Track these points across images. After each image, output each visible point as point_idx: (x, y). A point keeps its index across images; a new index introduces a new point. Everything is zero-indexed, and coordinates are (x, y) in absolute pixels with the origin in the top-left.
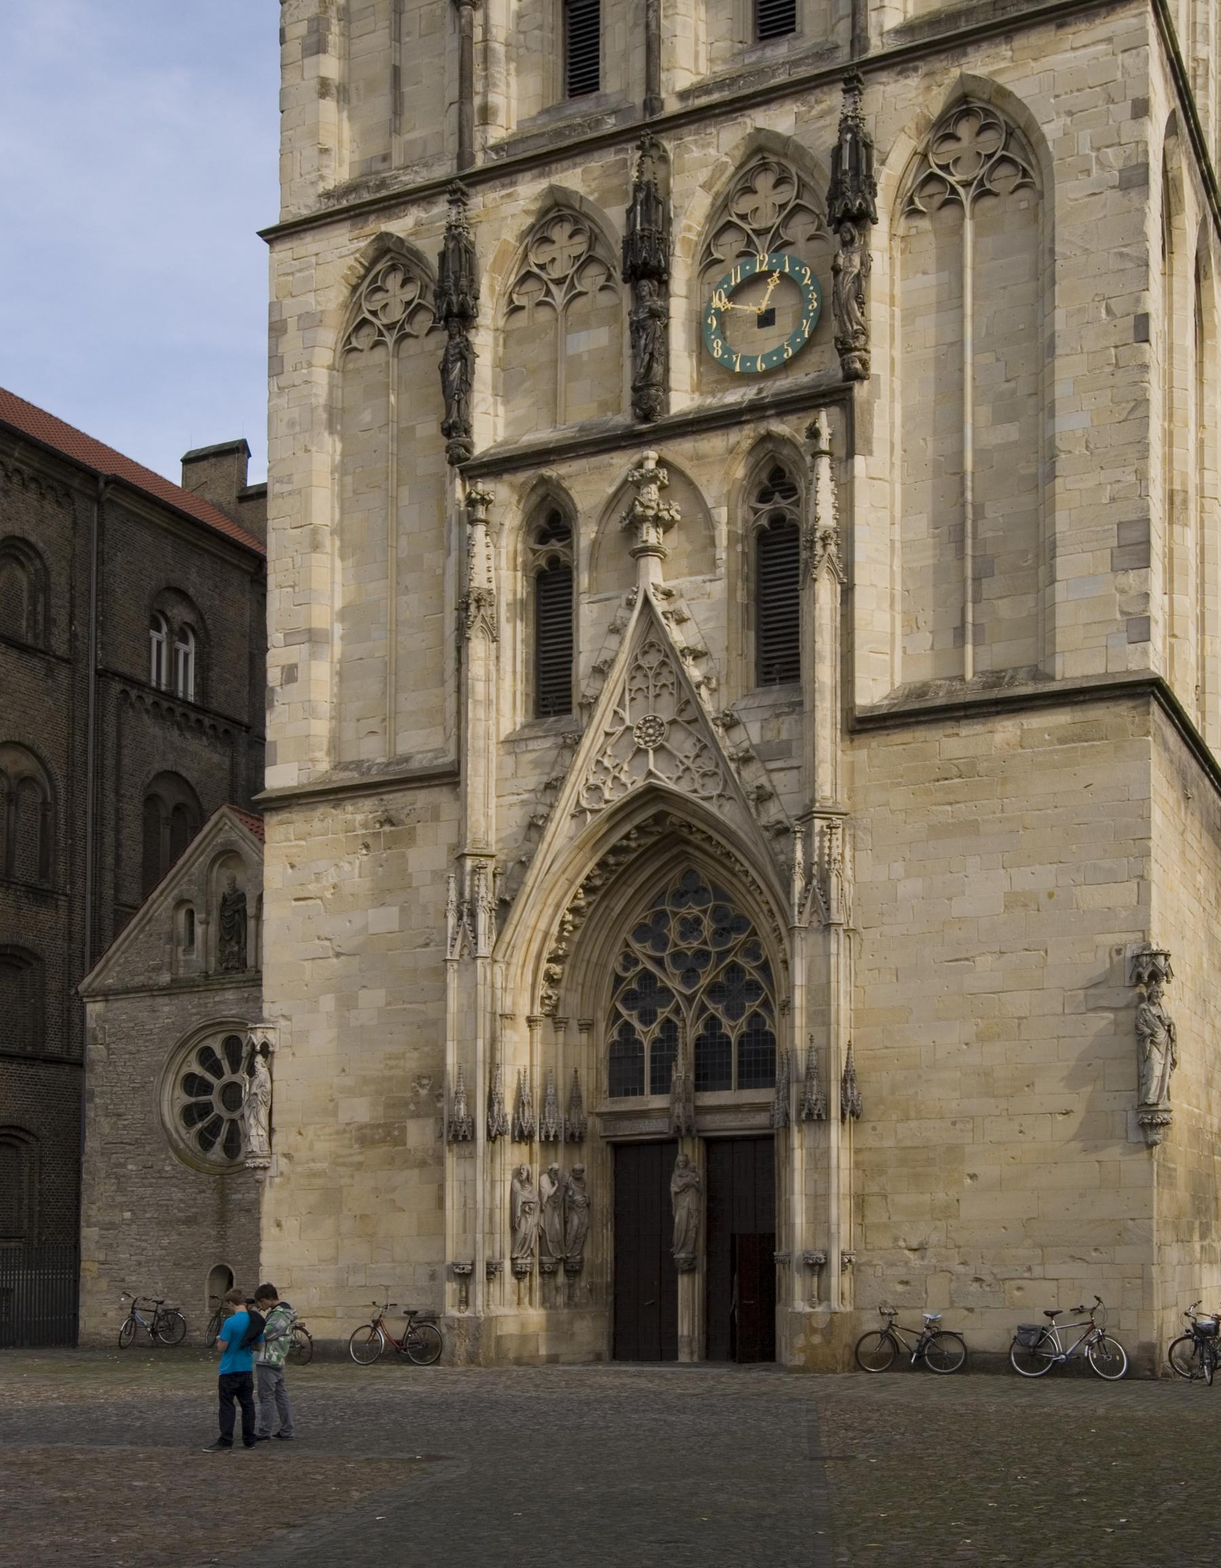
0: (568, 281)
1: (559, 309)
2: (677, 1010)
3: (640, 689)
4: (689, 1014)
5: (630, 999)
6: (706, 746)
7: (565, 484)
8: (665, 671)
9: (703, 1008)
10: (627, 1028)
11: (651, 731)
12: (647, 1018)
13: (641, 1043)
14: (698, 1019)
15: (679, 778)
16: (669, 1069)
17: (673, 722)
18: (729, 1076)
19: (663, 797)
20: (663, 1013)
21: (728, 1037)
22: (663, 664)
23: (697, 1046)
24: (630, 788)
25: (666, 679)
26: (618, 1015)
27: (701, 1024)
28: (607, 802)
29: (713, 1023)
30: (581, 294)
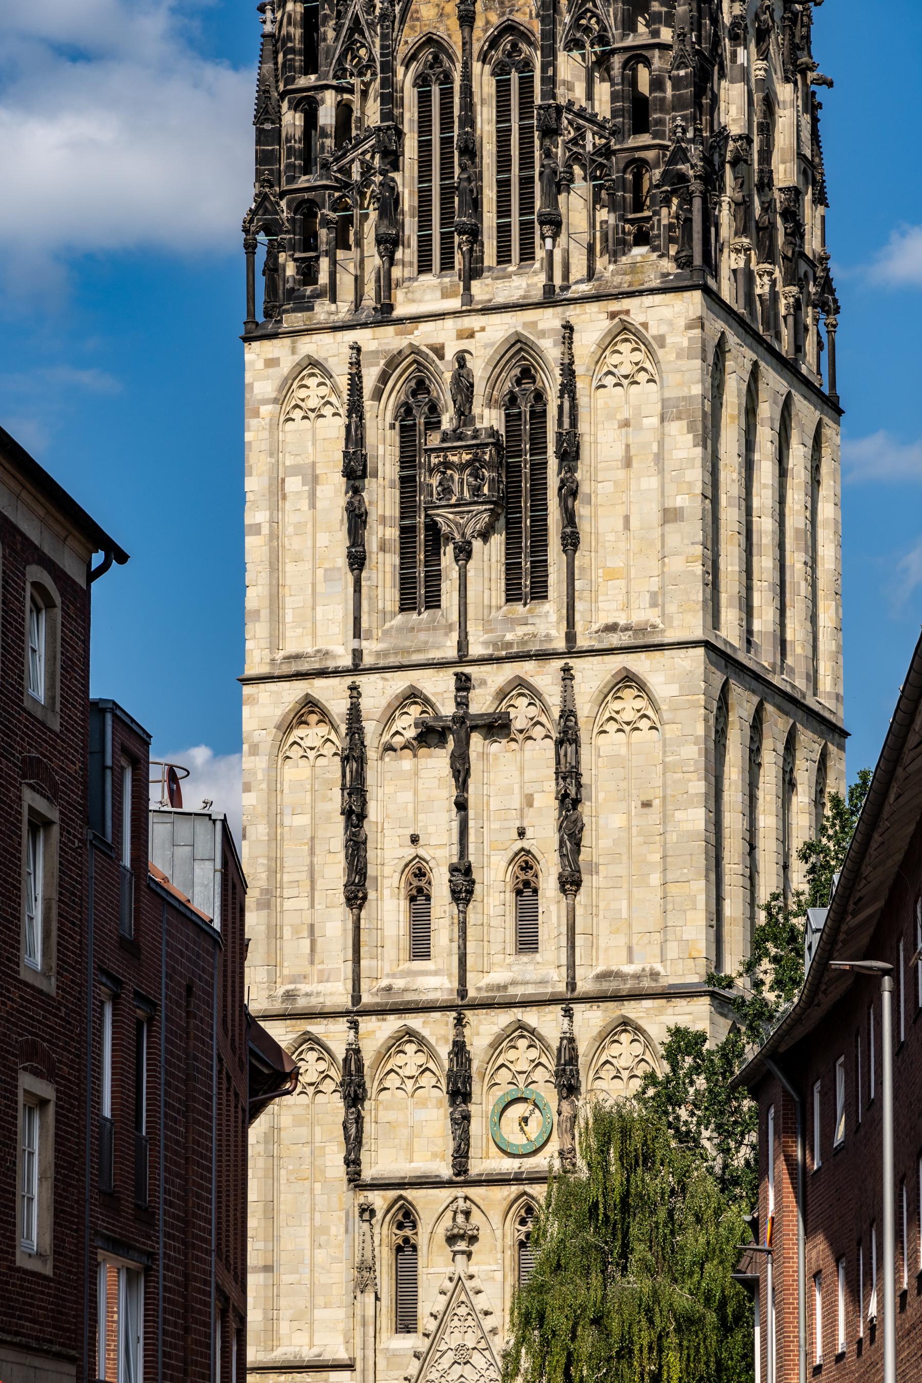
7: (414, 1203)
8: (469, 1317)
17: (474, 1349)
22: (469, 1314)
25: (470, 1322)
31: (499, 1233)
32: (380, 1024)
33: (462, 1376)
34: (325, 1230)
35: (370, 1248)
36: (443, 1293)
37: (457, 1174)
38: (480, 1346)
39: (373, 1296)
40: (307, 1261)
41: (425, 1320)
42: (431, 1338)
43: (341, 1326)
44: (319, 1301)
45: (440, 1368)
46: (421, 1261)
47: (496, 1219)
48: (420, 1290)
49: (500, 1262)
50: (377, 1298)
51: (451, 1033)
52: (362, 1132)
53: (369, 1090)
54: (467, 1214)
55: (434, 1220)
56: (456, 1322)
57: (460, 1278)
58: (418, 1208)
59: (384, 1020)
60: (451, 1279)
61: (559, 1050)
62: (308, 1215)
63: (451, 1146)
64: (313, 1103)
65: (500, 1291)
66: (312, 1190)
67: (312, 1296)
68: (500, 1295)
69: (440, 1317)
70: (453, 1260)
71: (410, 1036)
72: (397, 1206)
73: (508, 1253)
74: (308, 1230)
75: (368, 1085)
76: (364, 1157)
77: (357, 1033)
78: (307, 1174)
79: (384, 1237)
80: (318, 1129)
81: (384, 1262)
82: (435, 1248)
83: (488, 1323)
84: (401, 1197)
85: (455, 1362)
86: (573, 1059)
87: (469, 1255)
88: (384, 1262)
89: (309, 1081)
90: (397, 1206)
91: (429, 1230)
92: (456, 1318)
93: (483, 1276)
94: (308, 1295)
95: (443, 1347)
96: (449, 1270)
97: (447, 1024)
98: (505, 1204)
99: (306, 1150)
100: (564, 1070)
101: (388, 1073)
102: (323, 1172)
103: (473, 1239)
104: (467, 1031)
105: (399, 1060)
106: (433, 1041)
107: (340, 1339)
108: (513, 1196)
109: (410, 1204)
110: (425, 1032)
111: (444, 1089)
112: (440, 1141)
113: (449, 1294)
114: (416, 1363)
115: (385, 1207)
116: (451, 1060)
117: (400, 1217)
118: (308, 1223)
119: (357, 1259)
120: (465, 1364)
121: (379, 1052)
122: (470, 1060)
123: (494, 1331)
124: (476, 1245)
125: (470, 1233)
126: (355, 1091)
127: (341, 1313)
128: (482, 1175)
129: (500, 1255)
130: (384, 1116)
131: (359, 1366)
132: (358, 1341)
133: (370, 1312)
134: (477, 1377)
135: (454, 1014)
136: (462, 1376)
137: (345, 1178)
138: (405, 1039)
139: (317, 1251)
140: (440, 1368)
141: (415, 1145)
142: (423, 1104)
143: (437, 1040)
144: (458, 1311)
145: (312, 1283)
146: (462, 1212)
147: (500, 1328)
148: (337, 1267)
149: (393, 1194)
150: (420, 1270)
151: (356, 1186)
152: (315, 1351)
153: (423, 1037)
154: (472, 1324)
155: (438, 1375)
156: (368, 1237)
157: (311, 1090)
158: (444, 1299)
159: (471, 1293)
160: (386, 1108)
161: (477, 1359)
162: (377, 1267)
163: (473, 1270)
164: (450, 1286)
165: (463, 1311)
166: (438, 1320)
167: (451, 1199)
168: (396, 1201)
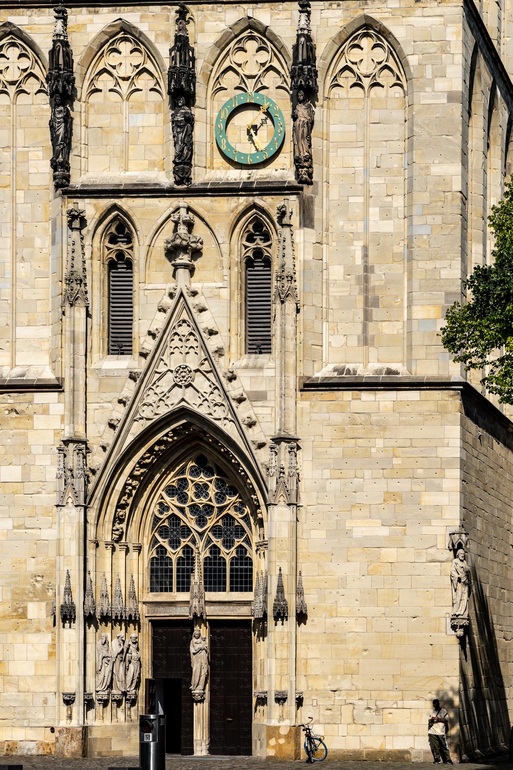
0: (130, 80)
1: (125, 98)
2: (194, 541)
3: (177, 347)
4: (201, 544)
5: (164, 532)
6: (218, 387)
7: (130, 213)
8: (192, 338)
9: (209, 541)
10: (162, 550)
11: (183, 374)
12: (174, 544)
13: (171, 559)
14: (206, 547)
15: (201, 405)
16: (189, 577)
18: (225, 583)
19: (189, 414)
20: (184, 541)
21: (224, 559)
22: (191, 334)
23: (205, 564)
24: (171, 408)
26: (156, 541)
27: (208, 550)
28: (156, 414)
29: (215, 550)
30: (138, 90)
31: (225, 248)
32: (91, 16)
33: (183, 400)
34: (28, 242)
35: (81, 259)
36: (163, 310)
37: (177, 183)
38: (203, 368)
39: (83, 311)
40: (9, 276)
41: (142, 339)
42: (149, 358)
43: (46, 346)
44: (22, 318)
45: (158, 391)
46: (137, 276)
47: (222, 233)
48: (136, 309)
49: (226, 278)
50: (88, 315)
51: (172, 29)
52: (71, 134)
53: (79, 90)
54: (190, 225)
55: (153, 231)
56: (176, 342)
57: (182, 295)
58: (134, 218)
59: (96, 12)
60: (171, 295)
61: (296, 48)
62: (9, 226)
63: (172, 152)
64: (14, 103)
65: (226, 310)
66: (14, 198)
67: (14, 312)
68: (226, 314)
69: (159, 335)
70: (174, 276)
71: (126, 32)
72: (110, 217)
73: (236, 269)
74: (9, 241)
75: (78, 84)
76: (73, 161)
77: (65, 24)
78: (8, 181)
79: (96, 250)
80: (20, 133)
81: (96, 277)
82: (153, 262)
83: (213, 343)
84: (115, 207)
85: (176, 385)
86: (311, 59)
87: (192, 270)
88: (96, 277)
89: (10, 79)
90: (110, 217)
91: (147, 243)
92: (176, 338)
93: (207, 294)
94: (9, 311)
95: (162, 369)
96: (169, 286)
97: (168, 19)
98: (232, 217)
99: (7, 155)
100: (301, 69)
101: (100, 73)
102: (26, 179)
103: (196, 253)
104: (190, 28)
105: (112, 59)
106: (152, 37)
107: (46, 359)
108: (241, 208)
109: (126, 214)
110: (143, 27)
111: (164, 90)
112: (158, 149)
113: (169, 311)
114: (132, 386)
115: (97, 216)
116: (173, 59)
117: (113, 230)
118: (10, 234)
119: (65, 271)
120: (187, 387)
121: (90, 48)
122: (193, 59)
123: (219, 352)
124: (199, 260)
125: (193, 245)
126: (64, 87)
127: (47, 332)
128: (207, 184)
129: (226, 271)
130: (94, 120)
131: (67, 386)
132: (67, 359)
133: (81, 328)
134: (200, 401)
135: (177, 8)
136: (183, 400)
137: (51, 184)
138: (120, 36)
139: (20, 265)
140: (158, 391)
141: (131, 153)
142: (140, 108)
143: (157, 36)
144: (179, 330)
145: (14, 299)
146: (184, 222)
147: (226, 349)
148: (41, 282)
149: (106, 203)
150: (135, 287)
151: (64, 193)
152: (17, 371)
153: (141, 33)
154: (195, 344)
155: (156, 398)
156: (78, 247)
157: (12, 90)
158: (163, 318)
159: (194, 311)
160: (98, 112)
161: (200, 382)
162: (88, 281)
163: (195, 286)
164: (170, 303)
165: (184, 330)
166: (157, 339)
167: (172, 209)
168: (109, 211)
